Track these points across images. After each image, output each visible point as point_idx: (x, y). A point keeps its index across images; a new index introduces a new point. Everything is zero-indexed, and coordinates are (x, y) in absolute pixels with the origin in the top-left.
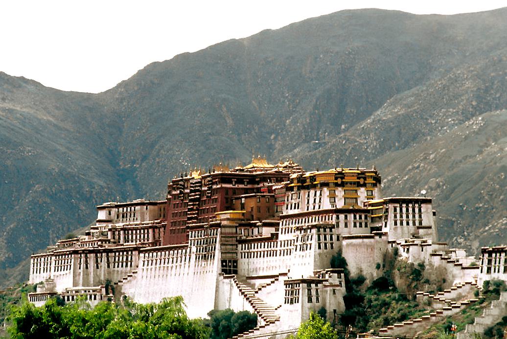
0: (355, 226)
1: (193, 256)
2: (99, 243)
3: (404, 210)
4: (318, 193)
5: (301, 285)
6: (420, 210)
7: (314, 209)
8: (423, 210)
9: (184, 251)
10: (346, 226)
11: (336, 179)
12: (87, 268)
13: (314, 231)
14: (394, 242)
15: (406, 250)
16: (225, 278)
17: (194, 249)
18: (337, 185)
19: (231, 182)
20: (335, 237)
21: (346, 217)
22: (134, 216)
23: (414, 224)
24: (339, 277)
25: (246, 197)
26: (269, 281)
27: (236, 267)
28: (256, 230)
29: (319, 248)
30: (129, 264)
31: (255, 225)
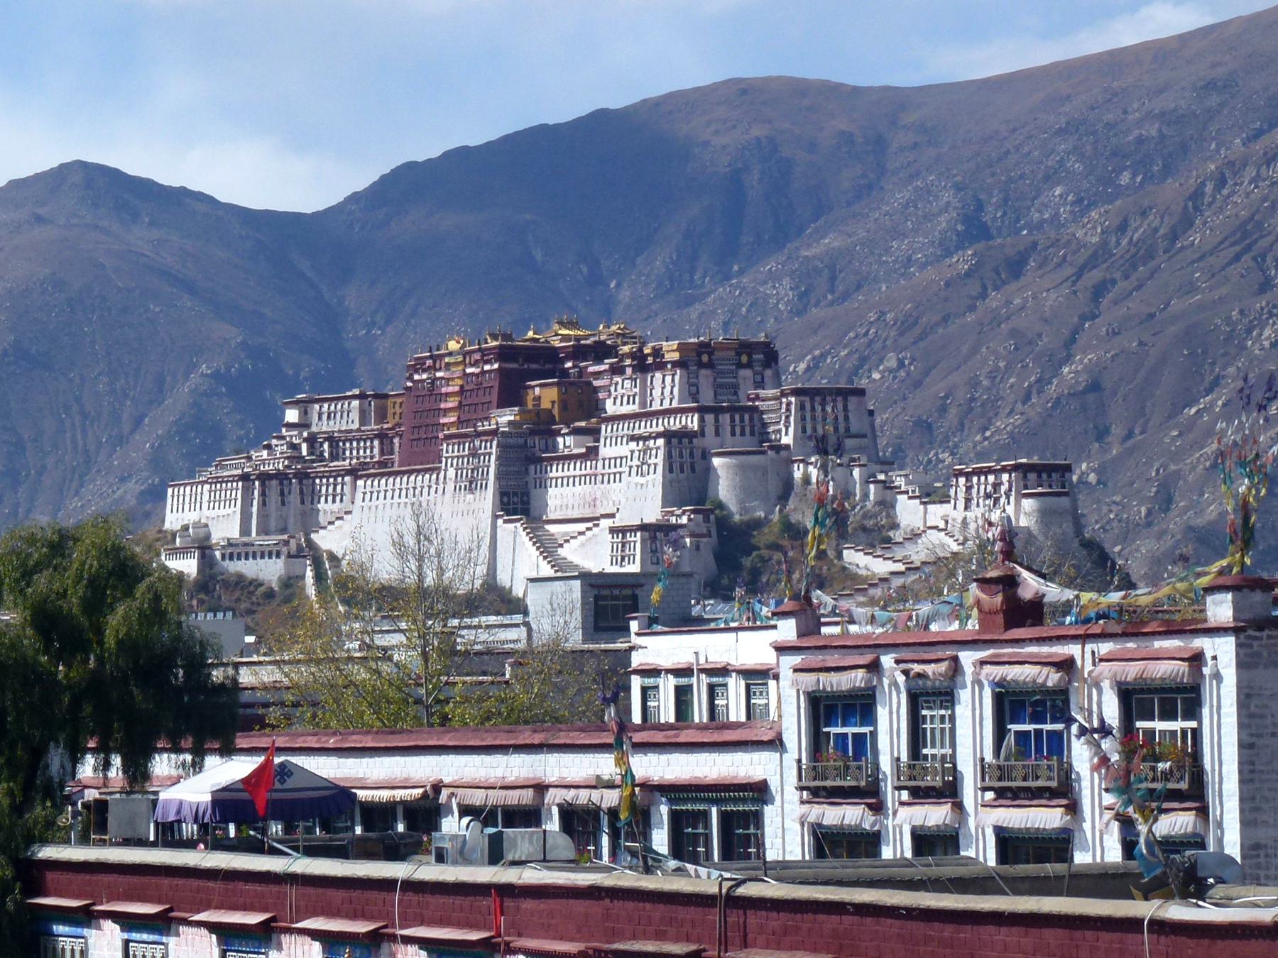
0: (733, 434)
1: (450, 486)
4: (668, 379)
5: (639, 534)
6: (845, 408)
8: (850, 407)
9: (434, 476)
10: (717, 434)
11: (699, 355)
13: (661, 442)
16: (505, 522)
18: (701, 365)
19: (516, 361)
20: (697, 453)
21: (717, 420)
24: (707, 520)
25: (541, 385)
26: (581, 527)
27: (528, 503)
29: (671, 471)
30: (338, 498)
31: (558, 433)
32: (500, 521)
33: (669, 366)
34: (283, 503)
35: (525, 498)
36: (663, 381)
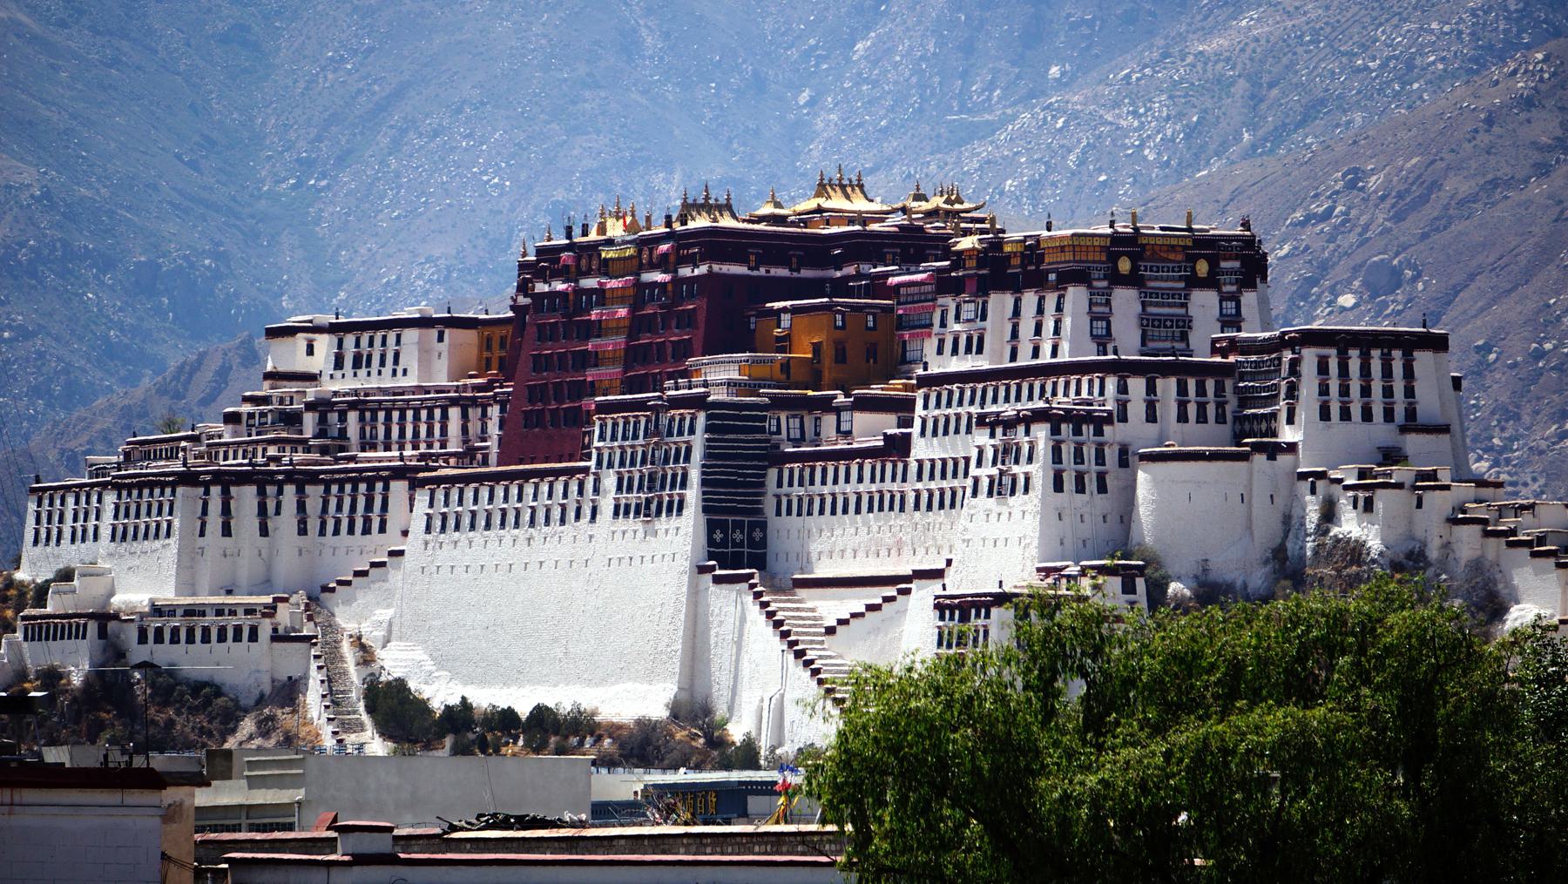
0: (1182, 417)
2: (272, 451)
3: (1354, 365)
5: (994, 611)
6: (1409, 373)
7: (1036, 354)
10: (1151, 417)
12: (227, 531)
13: (1041, 432)
14: (1321, 475)
15: (1361, 503)
16: (718, 580)
17: (609, 481)
18: (1117, 279)
20: (1111, 455)
21: (1151, 389)
22: (396, 361)
23: (1389, 415)
24: (1128, 588)
25: (795, 311)
26: (875, 595)
27: (763, 543)
28: (829, 421)
29: (1058, 486)
31: (826, 405)
32: (708, 577)
33: (1052, 277)
34: (264, 531)
35: (757, 534)
36: (1040, 310)
